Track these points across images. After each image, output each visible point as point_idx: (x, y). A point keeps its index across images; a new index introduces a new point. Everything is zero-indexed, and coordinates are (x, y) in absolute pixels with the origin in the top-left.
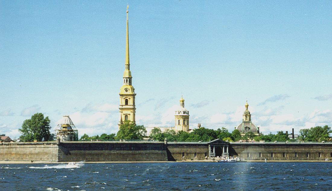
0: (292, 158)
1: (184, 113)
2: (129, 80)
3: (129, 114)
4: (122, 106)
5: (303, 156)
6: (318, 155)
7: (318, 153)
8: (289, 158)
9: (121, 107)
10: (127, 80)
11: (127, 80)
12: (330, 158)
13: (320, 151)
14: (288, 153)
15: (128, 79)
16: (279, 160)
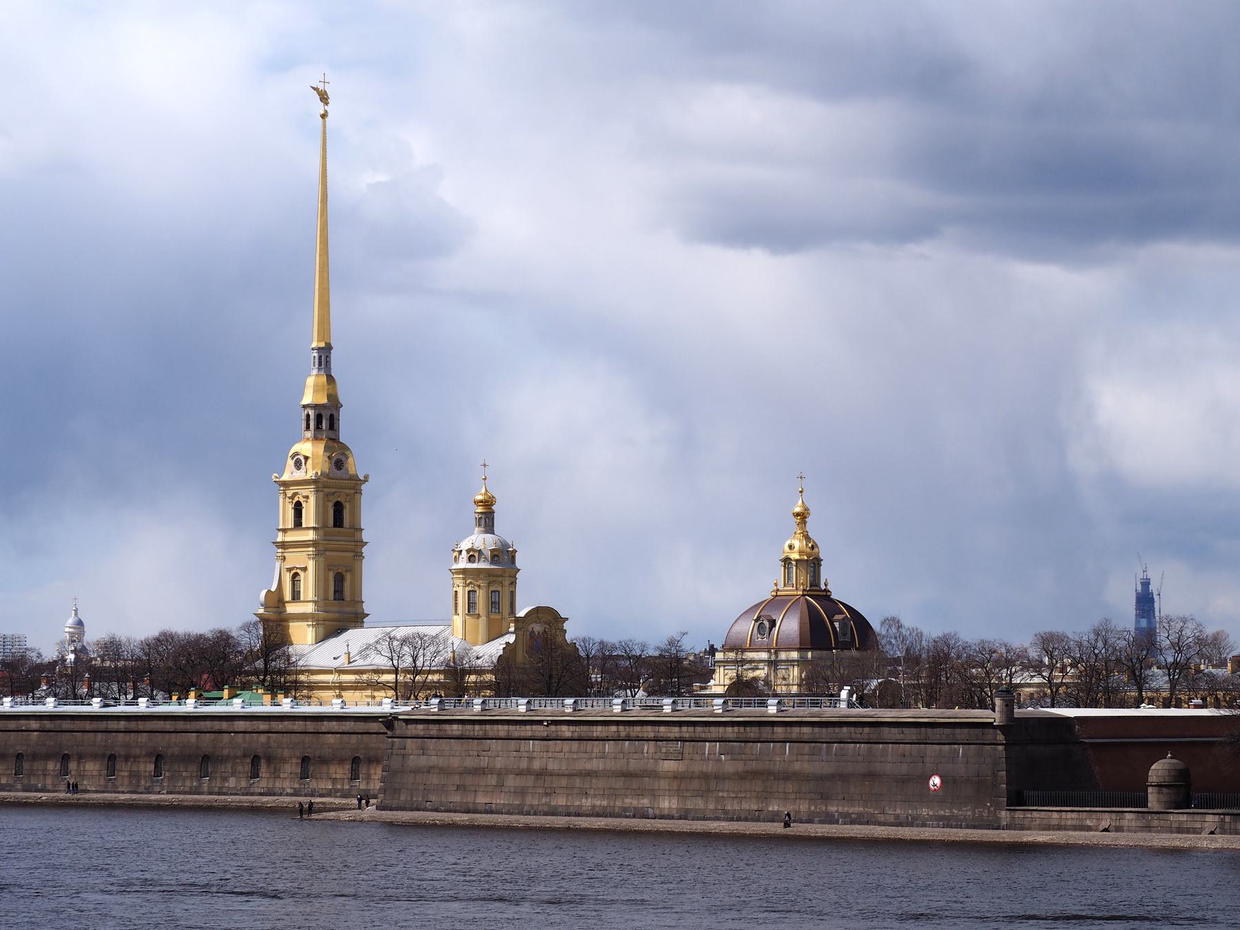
0: (143, 782)
1: (471, 559)
2: (325, 420)
3: (305, 569)
4: (285, 531)
5: (184, 774)
6: (248, 768)
7: (249, 760)
8: (126, 781)
9: (280, 538)
10: (308, 416)
11: (308, 416)
12: (297, 786)
13: (260, 752)
14: (127, 758)
15: (311, 413)
16: (88, 791)
